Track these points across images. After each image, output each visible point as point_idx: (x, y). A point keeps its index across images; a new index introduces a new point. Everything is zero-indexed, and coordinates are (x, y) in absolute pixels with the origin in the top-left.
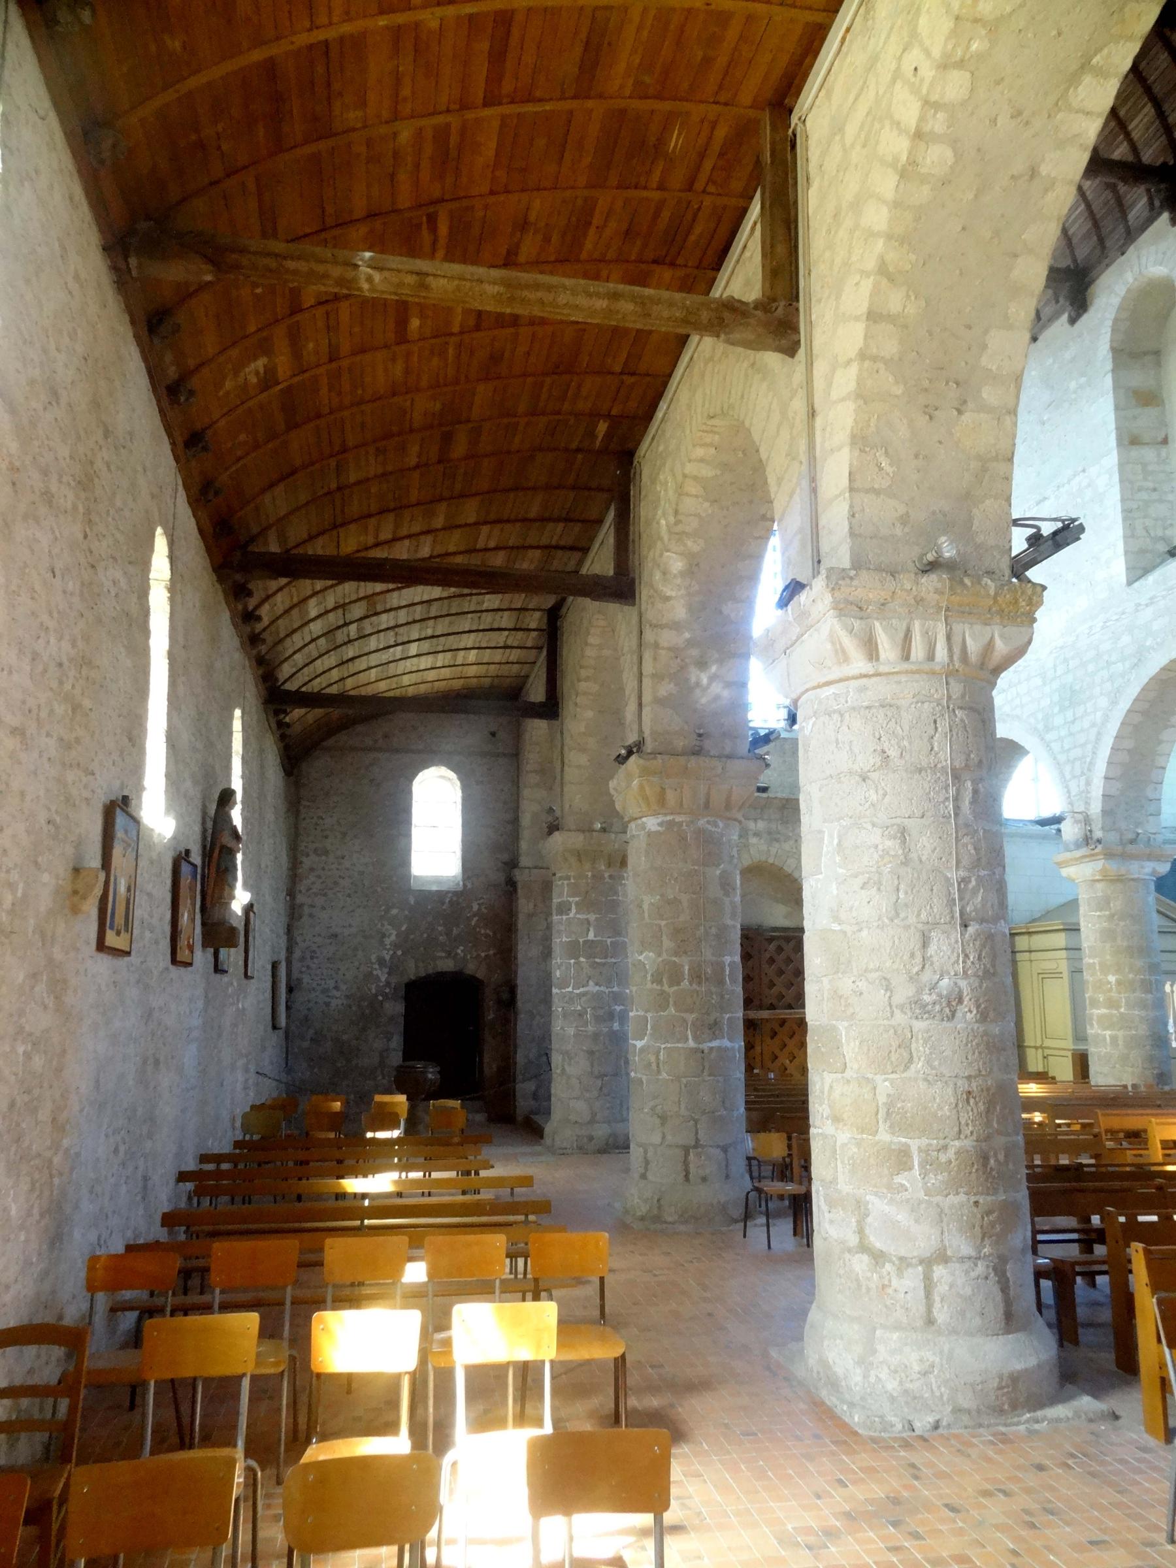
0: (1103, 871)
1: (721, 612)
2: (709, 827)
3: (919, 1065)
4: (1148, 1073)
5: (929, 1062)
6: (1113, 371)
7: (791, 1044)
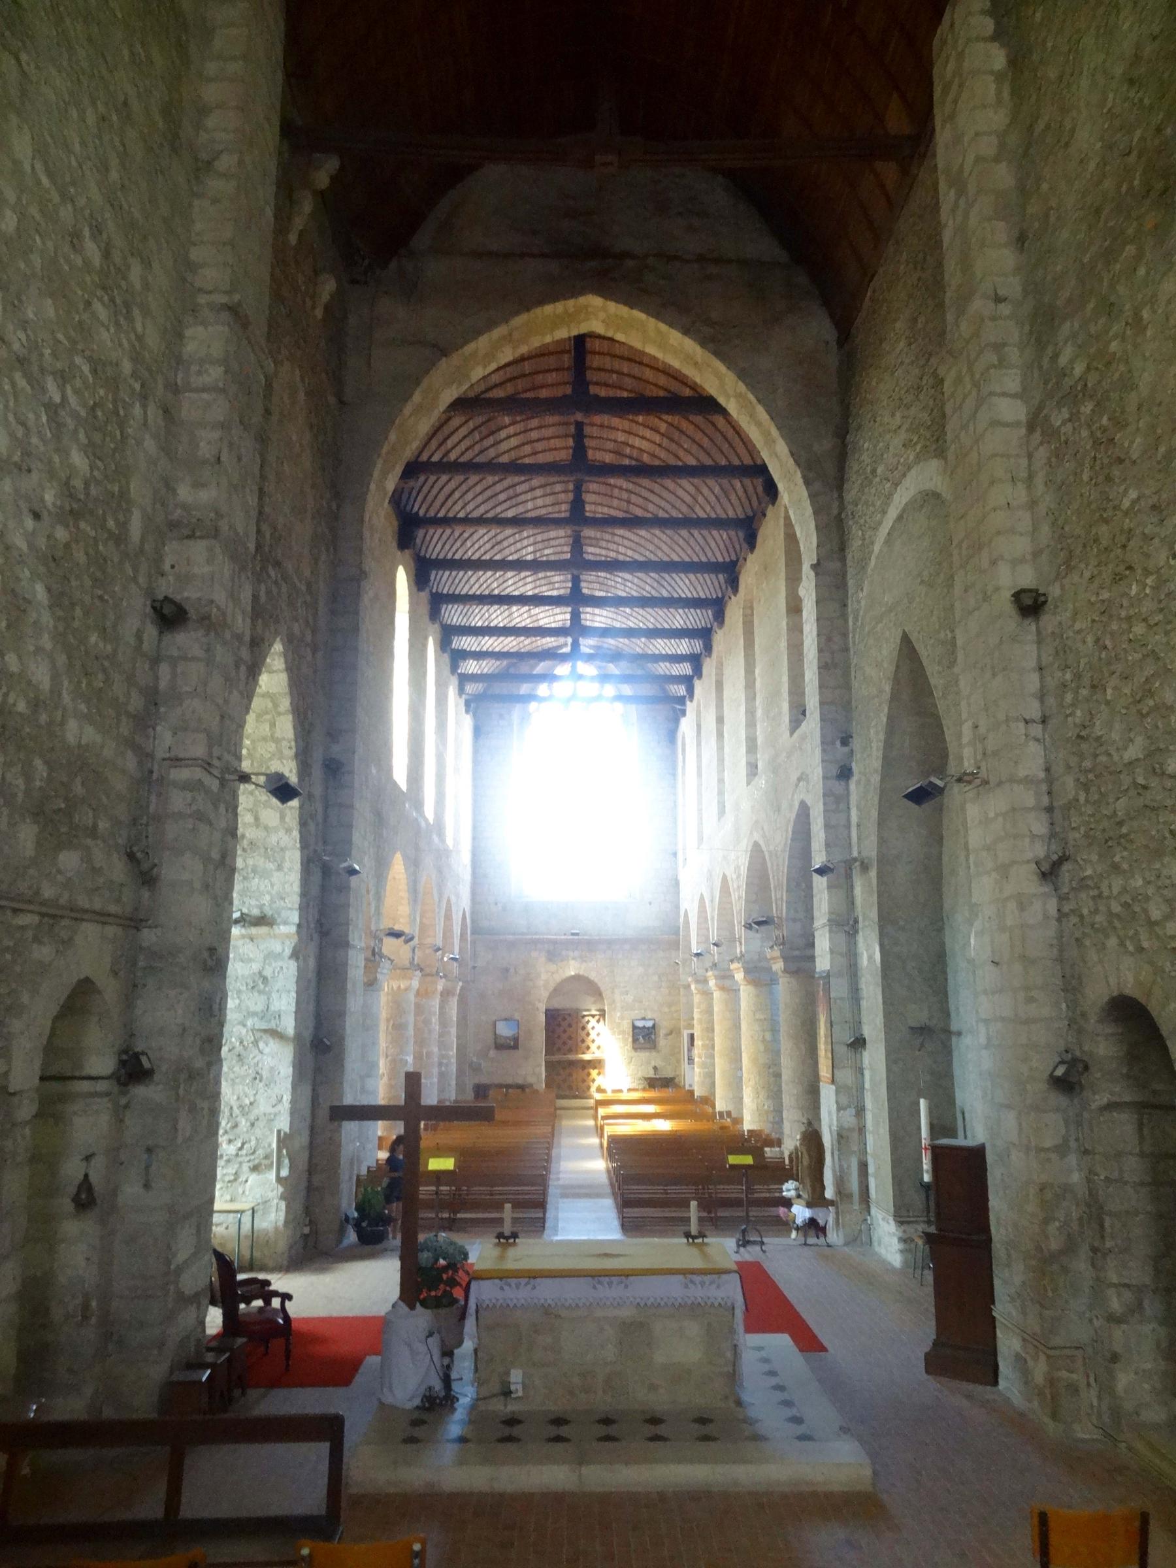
0: (696, 989)
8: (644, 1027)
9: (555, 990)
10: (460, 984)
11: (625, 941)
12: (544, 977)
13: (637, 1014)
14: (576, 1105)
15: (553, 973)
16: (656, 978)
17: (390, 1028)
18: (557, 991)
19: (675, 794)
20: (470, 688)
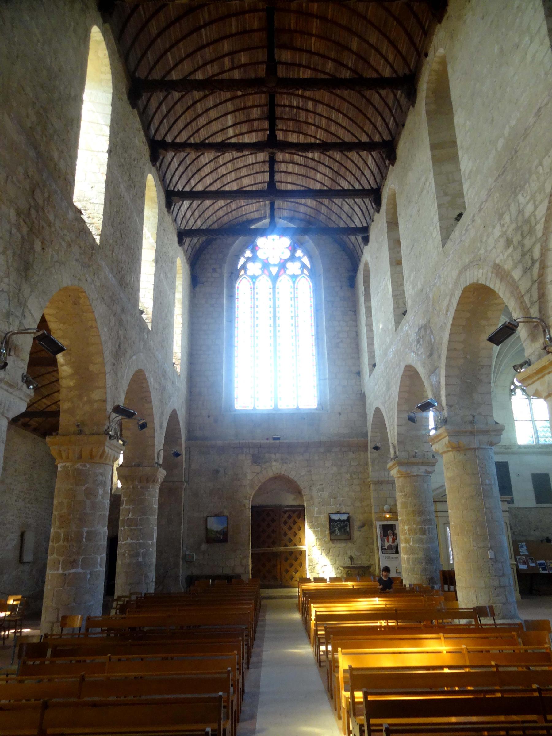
0: (399, 472)
1: (88, 369)
2: (81, 468)
4: (424, 578)
6: (387, 232)
7: (296, 564)
8: (339, 520)
9: (260, 489)
11: (320, 444)
12: (249, 477)
13: (332, 508)
14: (280, 594)
15: (258, 474)
16: (348, 476)
18: (261, 490)
19: (357, 326)
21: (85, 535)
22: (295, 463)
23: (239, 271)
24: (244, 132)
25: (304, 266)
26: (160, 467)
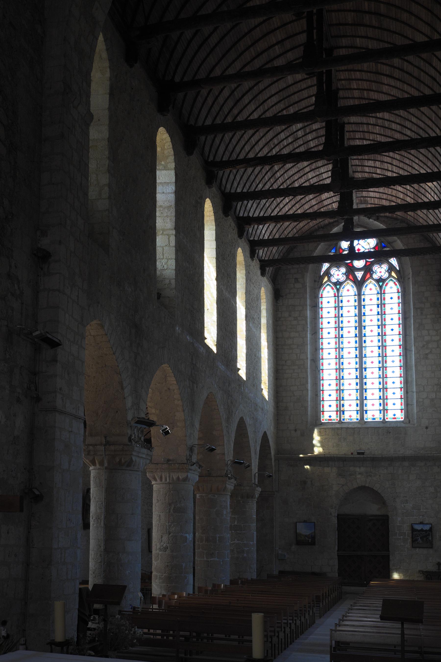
2: (212, 497)
3: (159, 560)
5: (161, 559)
8: (422, 530)
10: (259, 489)
15: (343, 485)
17: (172, 511)
20: (261, 252)
21: (218, 539)
22: (380, 476)
23: (322, 278)
24: (320, 166)
25: (391, 268)
26: (257, 487)
